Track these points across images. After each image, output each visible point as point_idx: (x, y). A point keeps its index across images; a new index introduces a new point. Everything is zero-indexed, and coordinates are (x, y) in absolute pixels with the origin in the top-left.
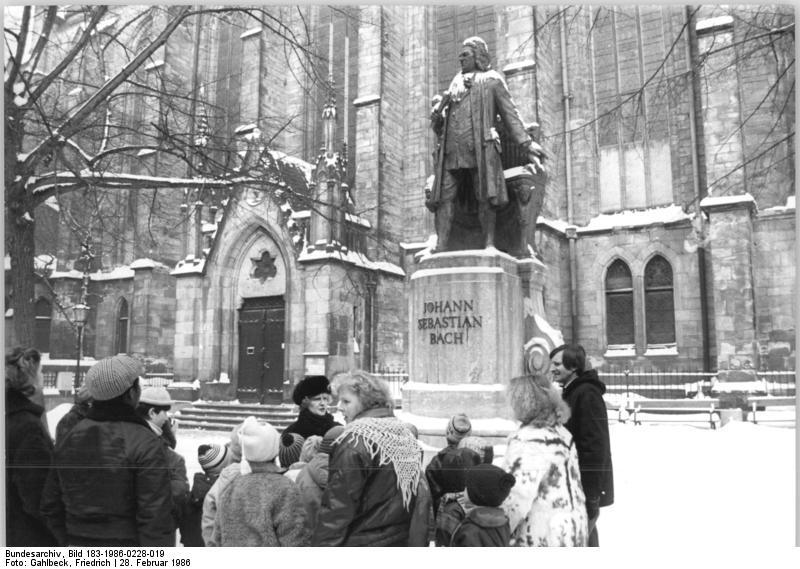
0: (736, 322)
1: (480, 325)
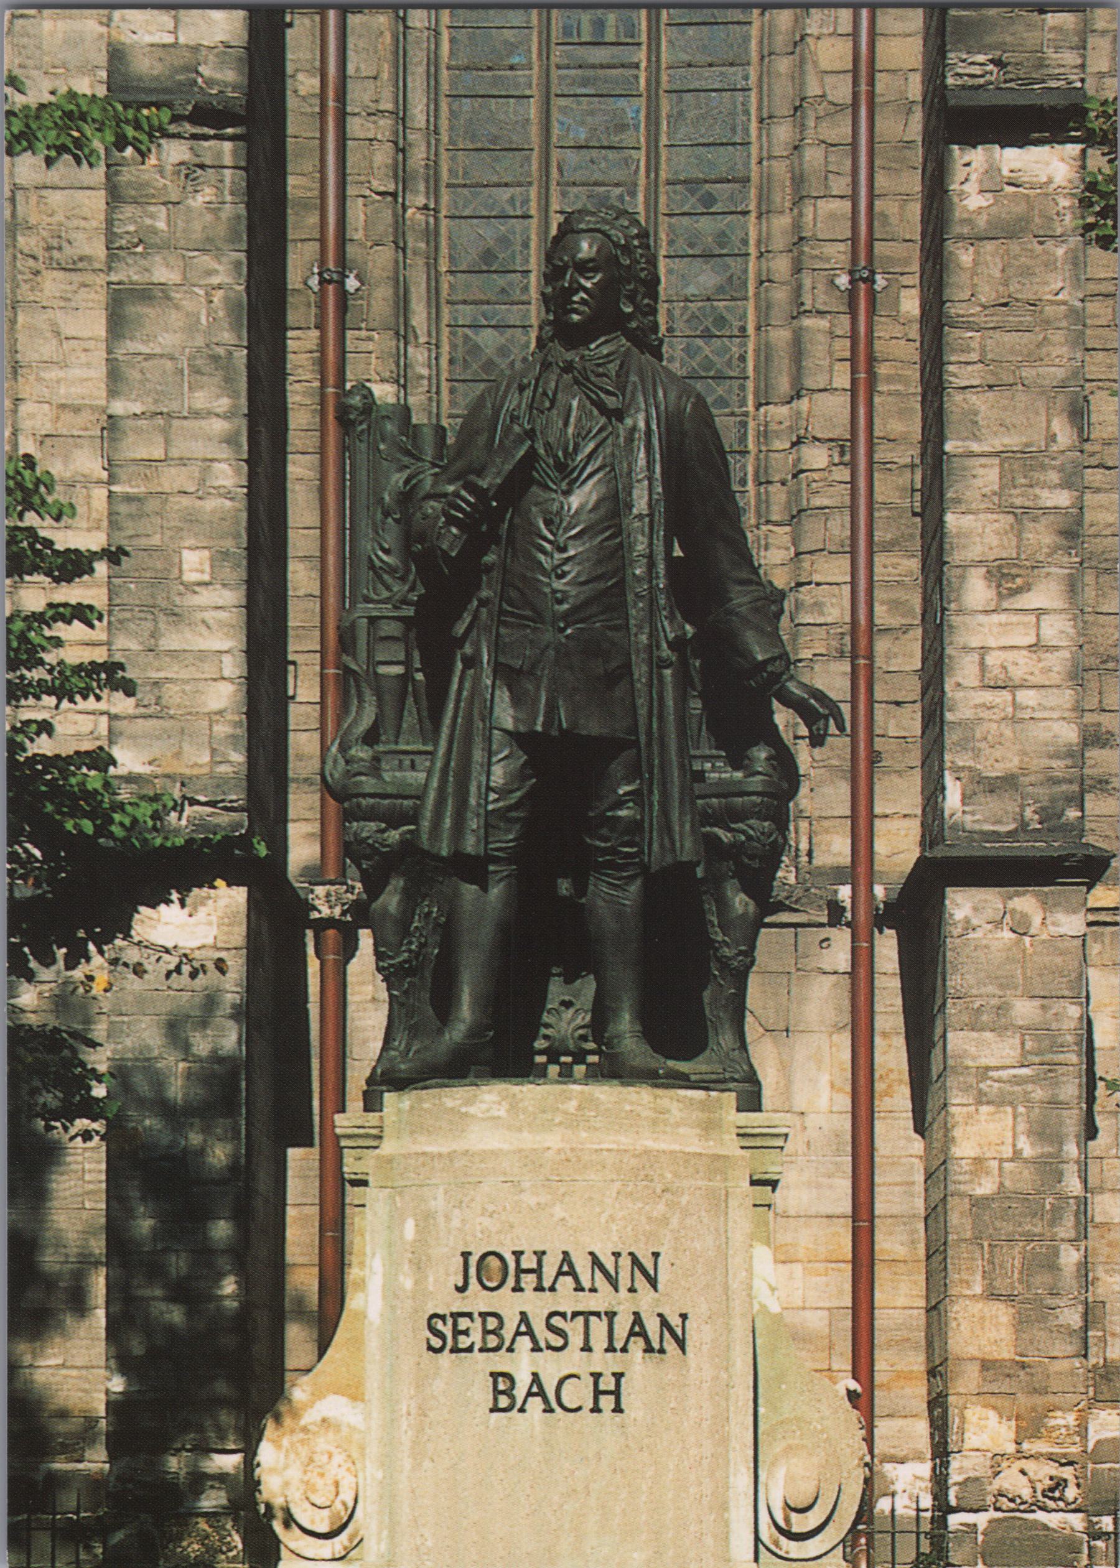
0: (1020, 1324)
1: (681, 1344)
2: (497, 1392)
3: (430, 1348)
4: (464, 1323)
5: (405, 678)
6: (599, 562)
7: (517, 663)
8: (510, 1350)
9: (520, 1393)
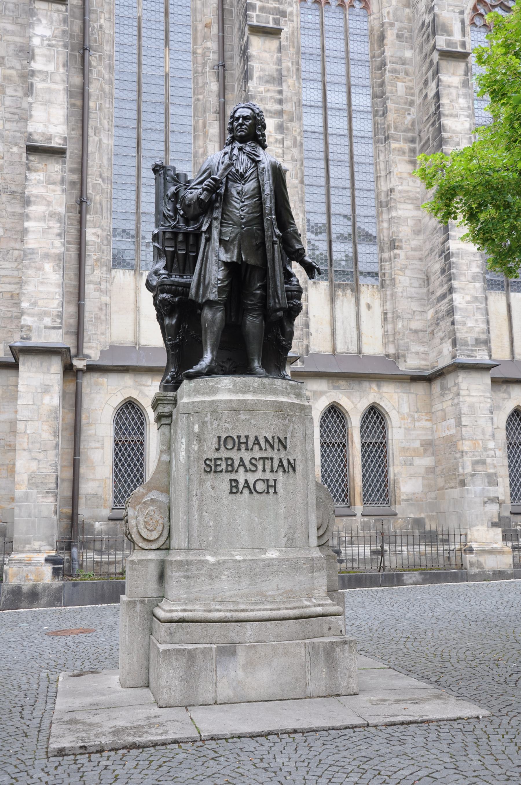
1: (294, 469)
2: (232, 487)
3: (205, 471)
4: (219, 462)
5: (174, 253)
6: (254, 208)
7: (227, 239)
8: (237, 471)
9: (241, 486)
